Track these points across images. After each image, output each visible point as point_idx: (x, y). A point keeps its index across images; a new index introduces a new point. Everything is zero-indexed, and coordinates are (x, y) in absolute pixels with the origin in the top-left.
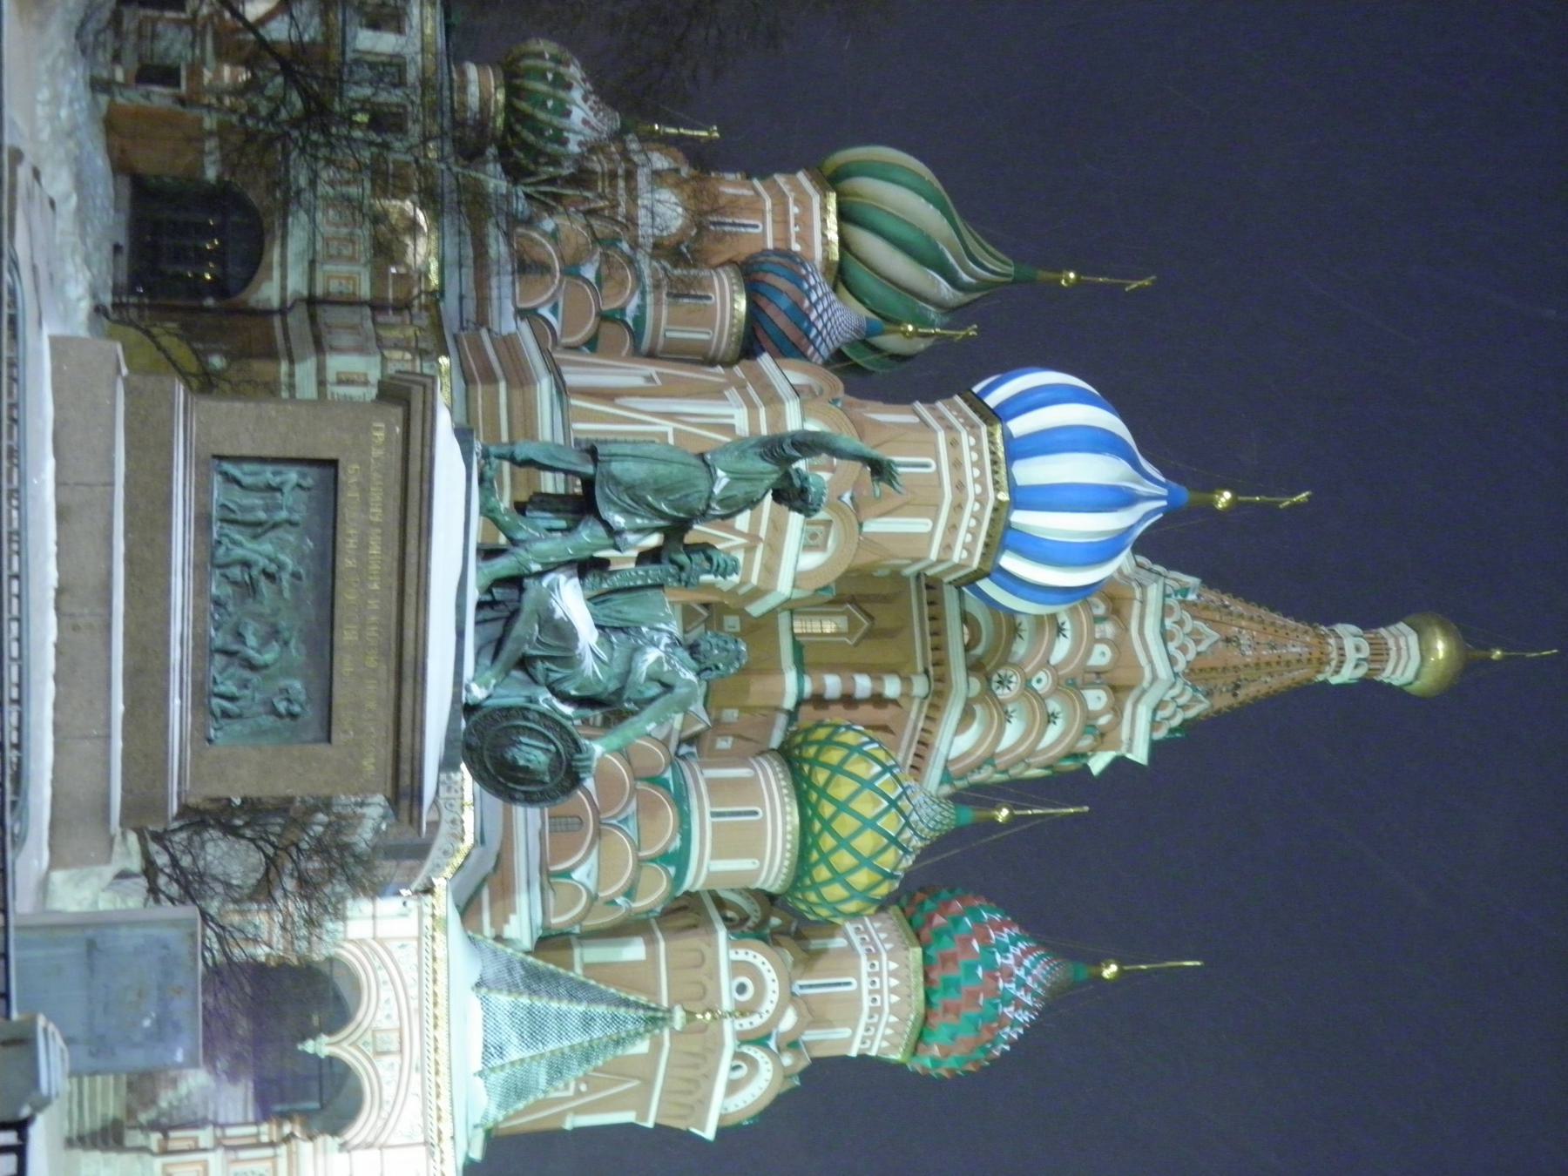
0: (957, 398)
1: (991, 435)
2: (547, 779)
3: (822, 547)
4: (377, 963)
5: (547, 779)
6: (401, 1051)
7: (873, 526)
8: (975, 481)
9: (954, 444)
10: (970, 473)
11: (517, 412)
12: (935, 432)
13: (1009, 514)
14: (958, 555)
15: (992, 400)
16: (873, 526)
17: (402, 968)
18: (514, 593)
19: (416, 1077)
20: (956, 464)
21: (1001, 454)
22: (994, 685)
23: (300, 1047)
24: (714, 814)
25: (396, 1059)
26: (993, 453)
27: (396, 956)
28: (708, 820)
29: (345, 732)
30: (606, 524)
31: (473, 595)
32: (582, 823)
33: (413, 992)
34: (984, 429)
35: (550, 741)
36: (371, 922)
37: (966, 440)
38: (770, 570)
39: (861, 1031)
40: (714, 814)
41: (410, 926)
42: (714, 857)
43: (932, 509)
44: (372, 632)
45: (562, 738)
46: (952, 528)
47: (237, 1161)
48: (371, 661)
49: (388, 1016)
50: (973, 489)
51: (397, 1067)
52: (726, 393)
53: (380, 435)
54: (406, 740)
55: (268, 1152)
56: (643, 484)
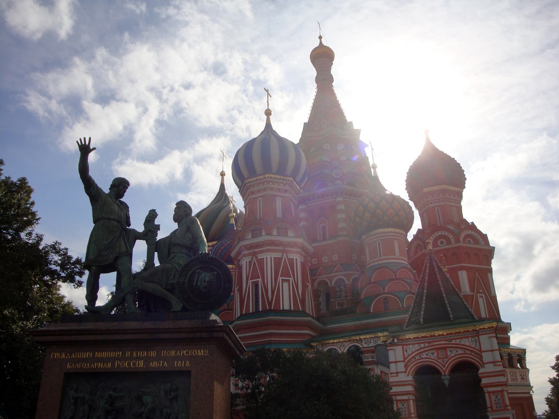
2: (215, 273)
4: (414, 360)
6: (445, 348)
9: (253, 193)
14: (287, 187)
17: (414, 350)
19: (453, 342)
21: (255, 179)
22: (338, 177)
23: (447, 386)
24: (381, 256)
25: (448, 350)
27: (410, 353)
28: (382, 257)
29: (185, 364)
32: (385, 298)
33: (422, 345)
34: (247, 185)
36: (398, 363)
39: (453, 204)
40: (381, 256)
41: (399, 349)
42: (394, 254)
44: (140, 354)
46: (279, 190)
47: (491, 407)
48: (153, 354)
49: (432, 354)
51: (451, 349)
53: (57, 355)
55: (487, 395)
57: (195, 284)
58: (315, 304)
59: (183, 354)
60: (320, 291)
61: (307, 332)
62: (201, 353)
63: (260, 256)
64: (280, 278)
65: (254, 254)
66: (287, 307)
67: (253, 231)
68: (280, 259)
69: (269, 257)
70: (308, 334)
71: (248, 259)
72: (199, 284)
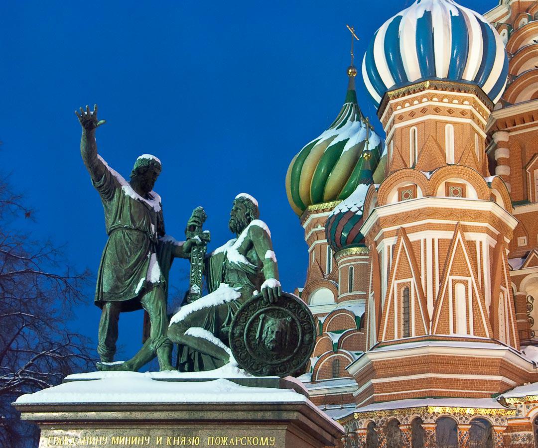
0: (381, 121)
1: (394, 97)
3: (463, 187)
5: (289, 319)
7: (451, 158)
8: (420, 102)
9: (401, 118)
10: (417, 106)
11: (407, 369)
12: (396, 129)
13: (439, 80)
14: (467, 107)
15: (378, 99)
16: (451, 158)
18: (185, 349)
20: (412, 114)
26: (404, 95)
30: (143, 292)
31: (176, 374)
34: (391, 102)
35: (257, 317)
37: (399, 111)
38: (478, 215)
43: (439, 126)
45: (255, 309)
46: (450, 112)
50: (426, 103)
52: (379, 252)
54: (241, 415)
56: (115, 271)
57: (257, 336)
58: (518, 325)
59: (239, 442)
60: (532, 298)
61: (500, 378)
62: (265, 441)
63: (412, 237)
64: (449, 278)
65: (404, 232)
66: (462, 332)
67: (400, 190)
68: (452, 241)
69: (427, 237)
70: (502, 382)
71: (389, 242)
72: (264, 336)
